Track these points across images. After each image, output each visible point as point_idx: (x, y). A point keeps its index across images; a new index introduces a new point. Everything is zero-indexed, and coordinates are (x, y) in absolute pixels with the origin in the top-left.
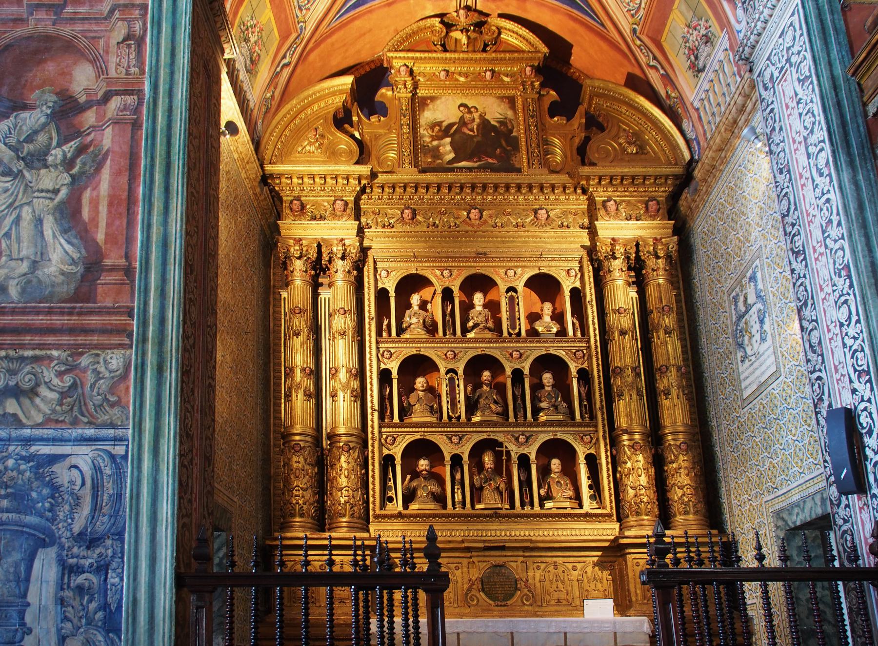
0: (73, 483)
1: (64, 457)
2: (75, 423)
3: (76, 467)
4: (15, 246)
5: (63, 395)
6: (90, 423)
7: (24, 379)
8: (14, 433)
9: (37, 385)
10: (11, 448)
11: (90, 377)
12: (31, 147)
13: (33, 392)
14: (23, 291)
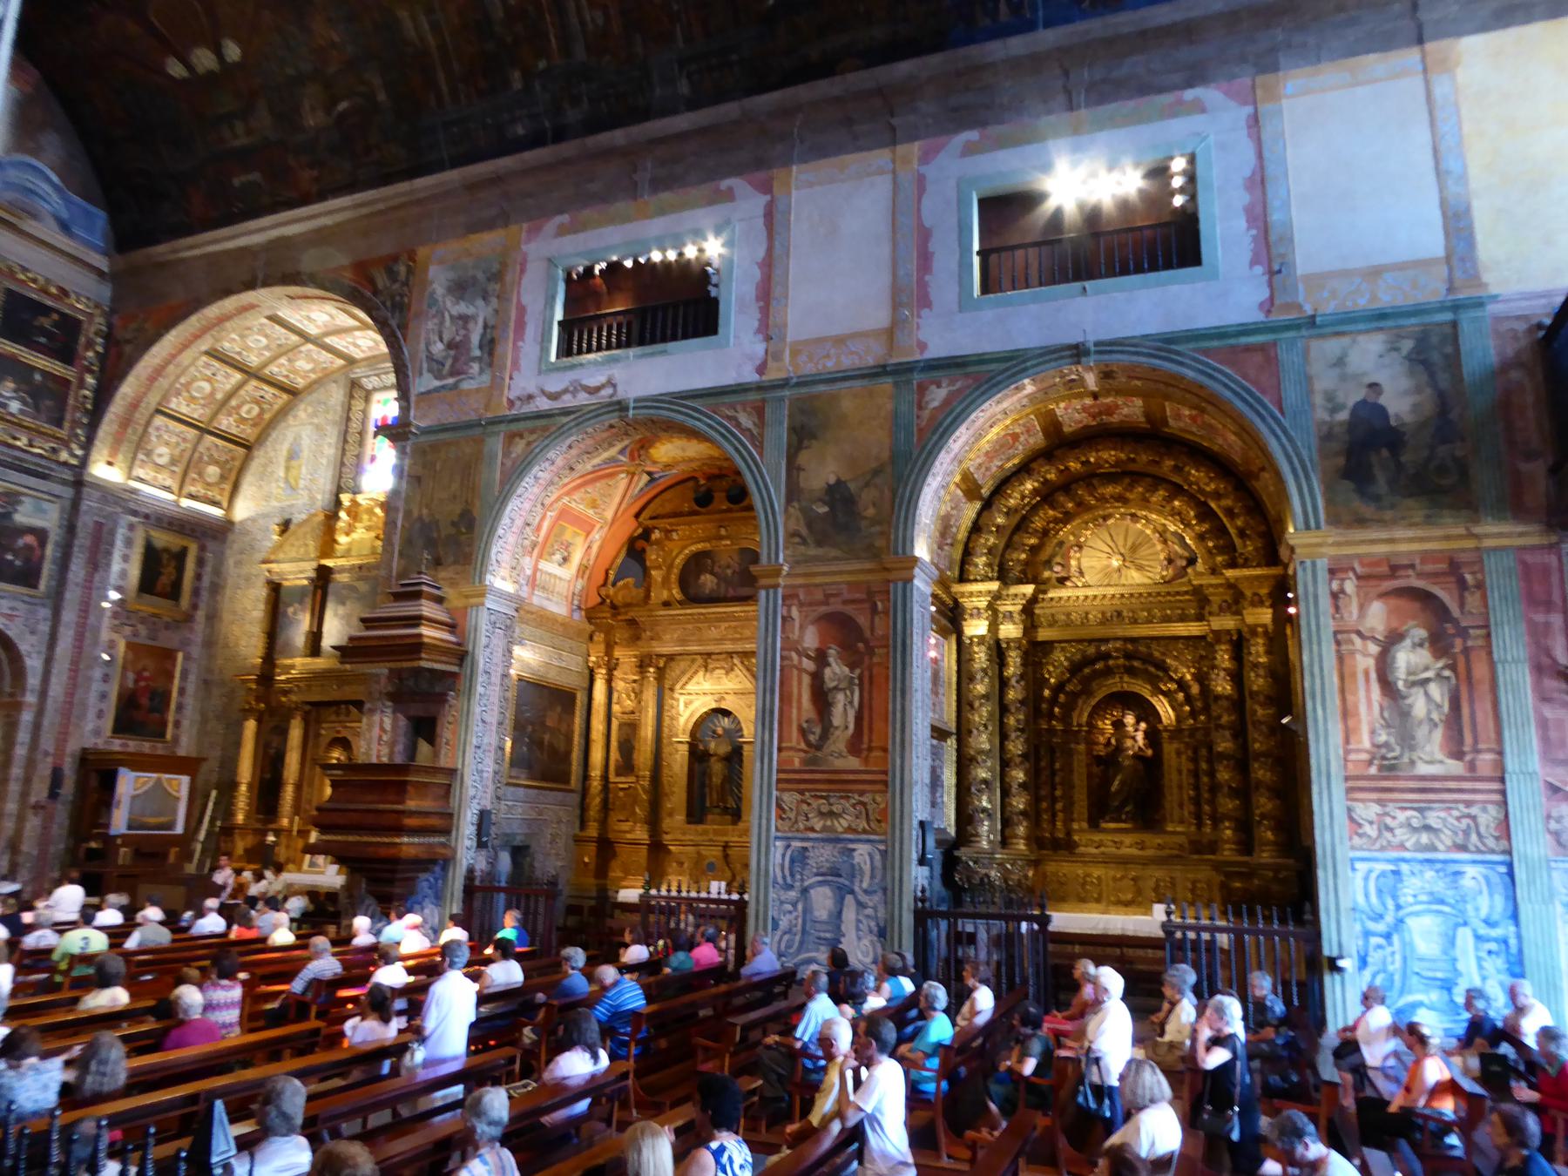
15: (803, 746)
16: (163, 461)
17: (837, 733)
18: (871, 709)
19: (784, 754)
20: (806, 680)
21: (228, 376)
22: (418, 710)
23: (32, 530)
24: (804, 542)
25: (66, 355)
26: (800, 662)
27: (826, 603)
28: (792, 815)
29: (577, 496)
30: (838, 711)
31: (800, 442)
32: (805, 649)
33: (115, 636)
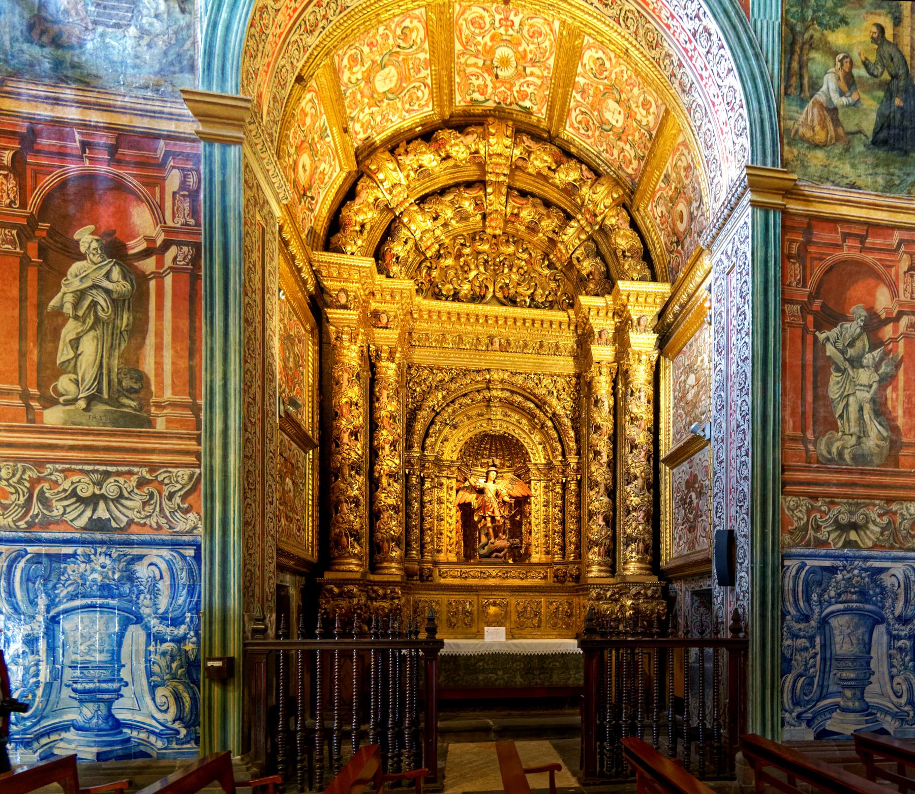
0: (893, 585)
1: (888, 569)
2: (892, 547)
3: (894, 575)
4: (846, 425)
5: (883, 529)
6: (900, 548)
7: (858, 518)
8: (857, 553)
9: (867, 522)
10: (856, 563)
11: (899, 519)
12: (852, 350)
13: (865, 527)
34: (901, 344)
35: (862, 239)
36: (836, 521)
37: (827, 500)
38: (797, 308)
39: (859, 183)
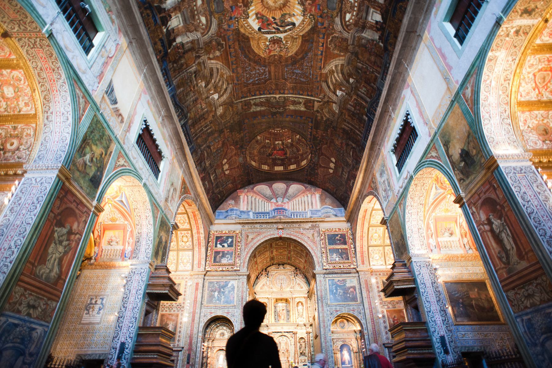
7: (36, 304)
11: (48, 308)
14: (45, 278)
15: (503, 265)
16: (378, 258)
17: (511, 252)
18: (517, 234)
19: (499, 273)
20: (489, 234)
21: (380, 230)
22: (413, 304)
23: (351, 287)
24: (464, 180)
25: (345, 243)
26: (484, 228)
27: (480, 198)
28: (516, 303)
29: (437, 211)
30: (506, 241)
31: (447, 146)
32: (483, 222)
33: (383, 309)
34: (74, 243)
35: (78, 204)
36: (29, 303)
37: (30, 292)
38: (53, 215)
39: (84, 188)
